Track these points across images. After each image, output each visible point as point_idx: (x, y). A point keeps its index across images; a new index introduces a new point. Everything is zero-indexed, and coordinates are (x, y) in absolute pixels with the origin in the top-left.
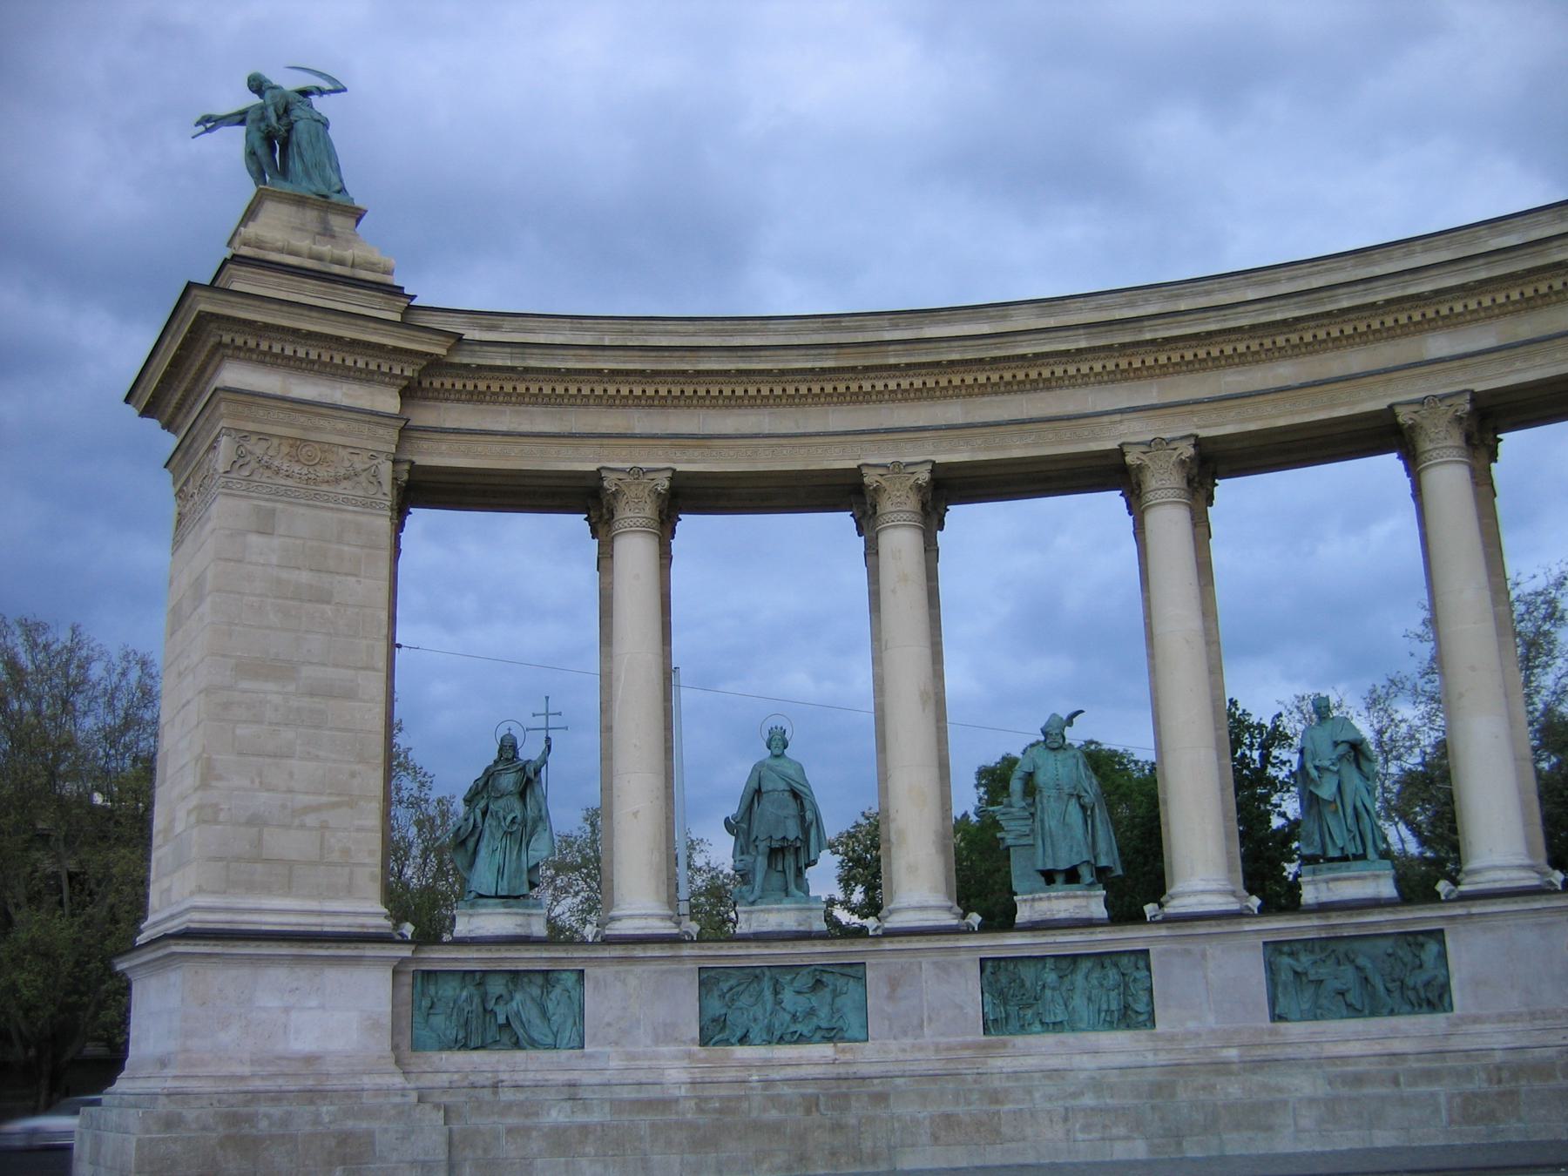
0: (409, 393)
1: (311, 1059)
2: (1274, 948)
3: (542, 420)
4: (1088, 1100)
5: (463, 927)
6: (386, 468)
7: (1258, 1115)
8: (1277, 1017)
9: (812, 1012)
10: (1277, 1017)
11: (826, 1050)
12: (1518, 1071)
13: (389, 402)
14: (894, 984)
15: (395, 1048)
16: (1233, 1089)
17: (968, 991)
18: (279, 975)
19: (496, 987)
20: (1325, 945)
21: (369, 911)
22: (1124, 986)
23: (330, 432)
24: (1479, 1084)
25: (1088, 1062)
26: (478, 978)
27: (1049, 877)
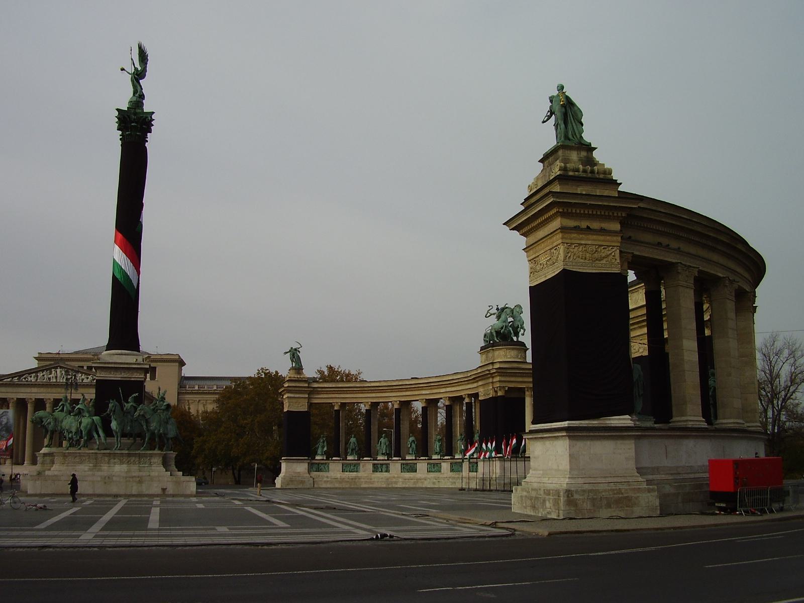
1: (299, 472)
3: (325, 396)
4: (381, 480)
5: (316, 458)
6: (307, 404)
7: (396, 483)
9: (354, 469)
10: (401, 472)
11: (355, 473)
12: (419, 479)
13: (307, 396)
14: (363, 466)
16: (394, 480)
17: (371, 467)
18: (295, 464)
19: (320, 465)
20: (407, 464)
22: (387, 467)
23: (300, 400)
24: (415, 480)
25: (382, 476)
26: (318, 464)
27: (382, 454)
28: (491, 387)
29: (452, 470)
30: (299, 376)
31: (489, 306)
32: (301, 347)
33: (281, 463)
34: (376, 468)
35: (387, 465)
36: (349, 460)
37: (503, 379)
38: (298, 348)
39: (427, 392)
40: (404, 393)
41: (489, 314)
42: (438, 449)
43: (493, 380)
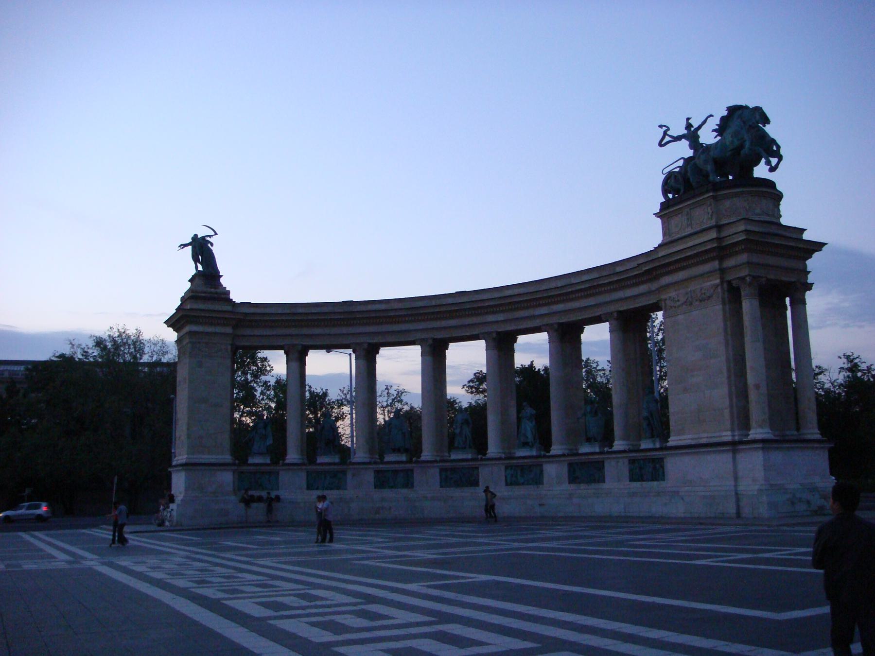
0: (235, 327)
2: (442, 470)
3: (268, 332)
6: (229, 347)
8: (441, 487)
10: (441, 487)
14: (354, 475)
15: (234, 490)
20: (453, 470)
21: (227, 458)
28: (718, 281)
29: (573, 479)
30: (213, 290)
31: (661, 126)
32: (216, 234)
33: (170, 473)
34: (383, 480)
35: (409, 473)
36: (322, 464)
37: (755, 258)
38: (210, 236)
39: (500, 317)
40: (444, 323)
41: (667, 139)
42: (529, 435)
43: (720, 264)
